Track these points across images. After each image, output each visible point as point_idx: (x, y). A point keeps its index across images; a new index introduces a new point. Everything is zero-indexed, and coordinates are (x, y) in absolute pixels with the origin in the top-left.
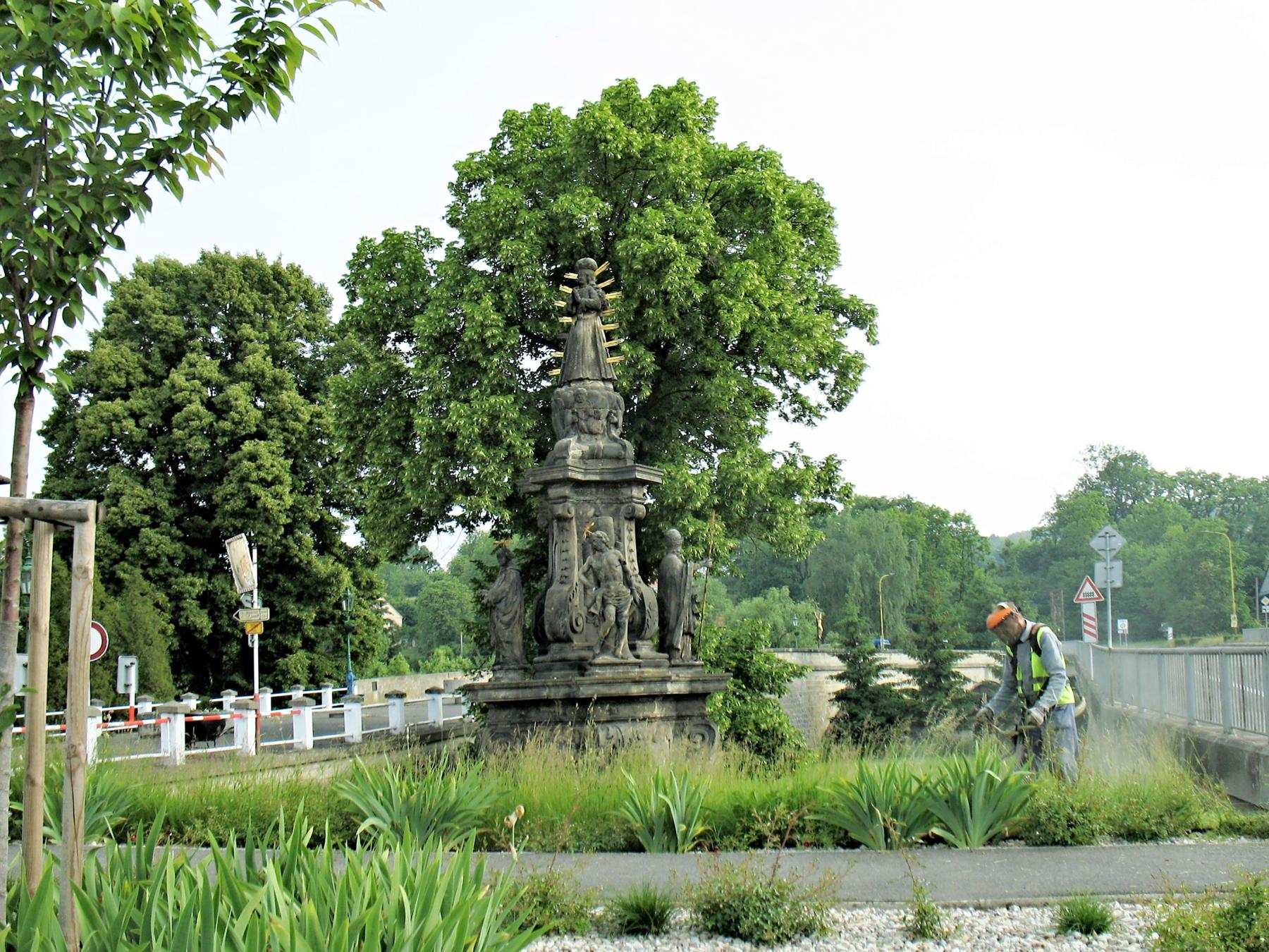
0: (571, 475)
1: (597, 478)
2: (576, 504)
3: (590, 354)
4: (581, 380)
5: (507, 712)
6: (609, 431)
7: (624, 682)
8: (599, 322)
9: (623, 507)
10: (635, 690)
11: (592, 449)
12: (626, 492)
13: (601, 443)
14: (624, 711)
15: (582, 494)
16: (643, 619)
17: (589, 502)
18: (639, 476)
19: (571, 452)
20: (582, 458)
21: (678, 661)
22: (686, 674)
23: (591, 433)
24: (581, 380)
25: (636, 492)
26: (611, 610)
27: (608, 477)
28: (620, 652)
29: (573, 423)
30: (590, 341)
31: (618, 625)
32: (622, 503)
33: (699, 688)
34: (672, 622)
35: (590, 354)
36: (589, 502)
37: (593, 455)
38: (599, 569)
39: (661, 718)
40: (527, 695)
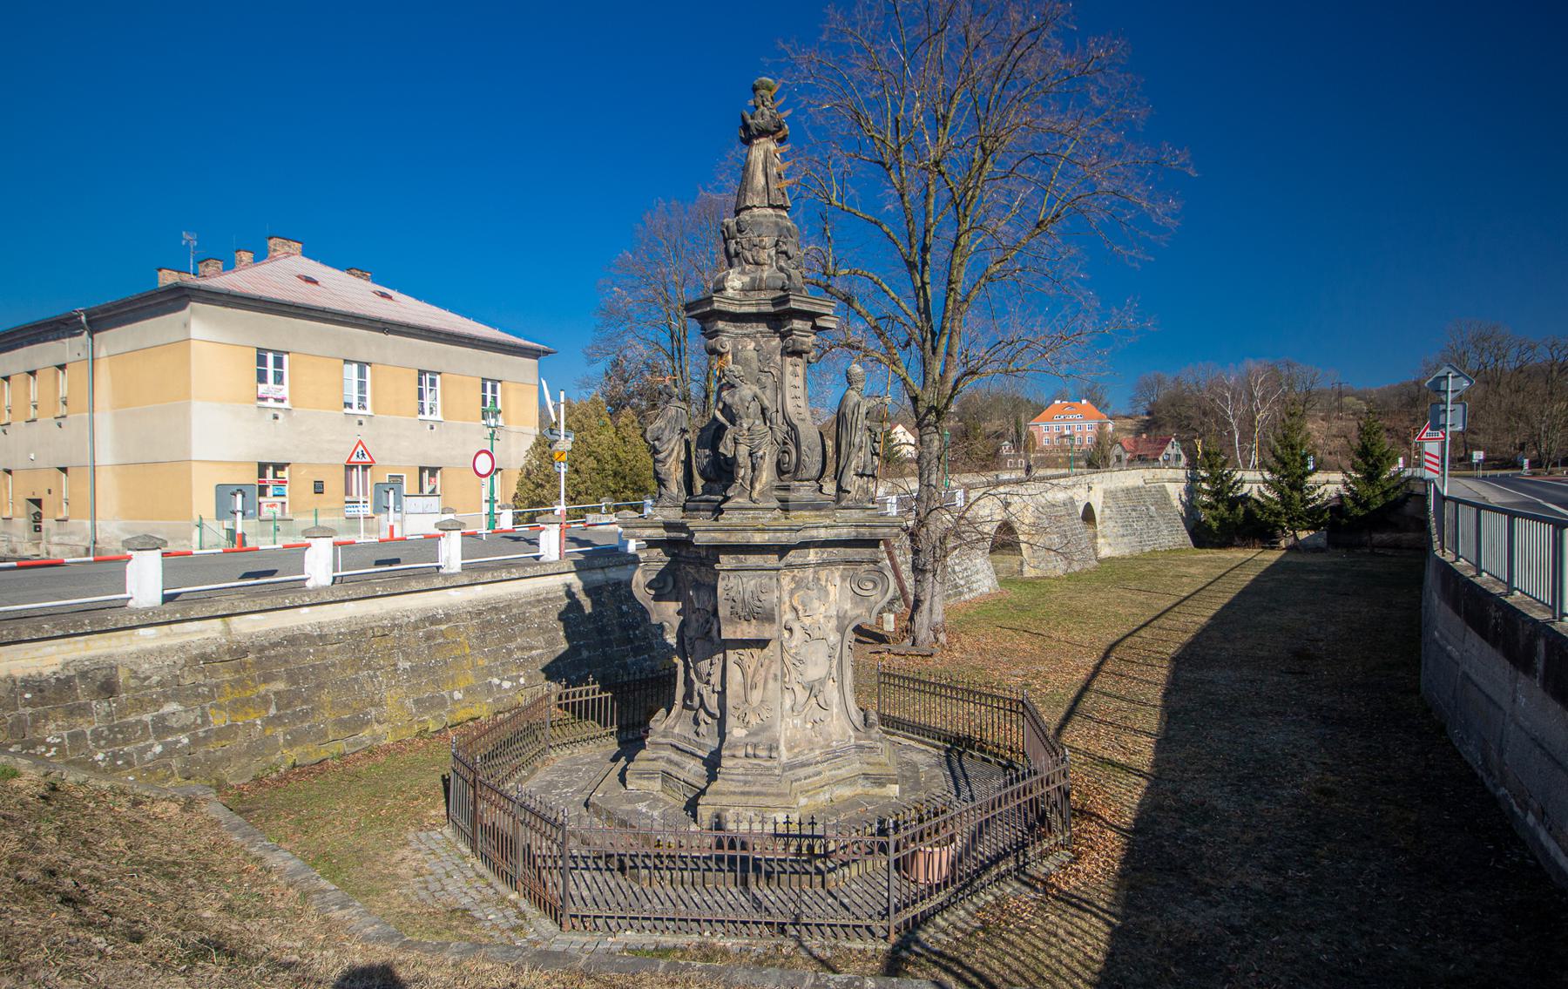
0: (716, 305)
1: (754, 310)
3: (760, 180)
4: (748, 208)
8: (772, 147)
13: (766, 273)
17: (748, 336)
18: (793, 305)
22: (856, 515)
24: (748, 208)
25: (797, 324)
28: (755, 495)
29: (737, 254)
35: (760, 180)
36: (748, 336)
39: (819, 565)
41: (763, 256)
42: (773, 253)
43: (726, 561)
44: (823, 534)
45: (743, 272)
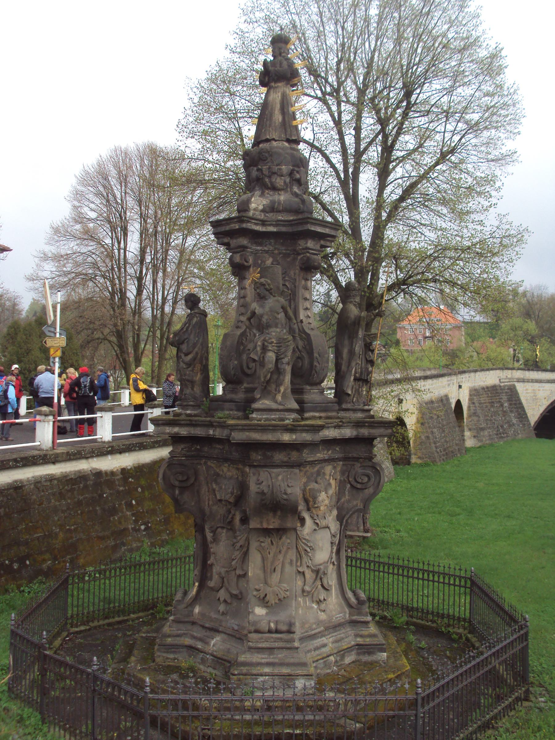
2: (255, 253)
4: (267, 140)
5: (182, 446)
6: (291, 188)
7: (275, 428)
9: (299, 257)
10: (286, 437)
11: (273, 202)
12: (302, 244)
13: (282, 197)
14: (279, 457)
15: (260, 244)
16: (311, 365)
17: (267, 252)
19: (253, 206)
20: (263, 211)
21: (349, 406)
23: (274, 189)
24: (267, 140)
26: (271, 356)
27: (284, 229)
30: (278, 106)
31: (278, 371)
32: (299, 254)
33: (365, 432)
34: (344, 368)
36: (267, 252)
37: (272, 208)
38: (262, 316)
40: (199, 432)
41: (279, 182)
42: (288, 180)
43: (256, 456)
44: (331, 433)
45: (262, 195)
